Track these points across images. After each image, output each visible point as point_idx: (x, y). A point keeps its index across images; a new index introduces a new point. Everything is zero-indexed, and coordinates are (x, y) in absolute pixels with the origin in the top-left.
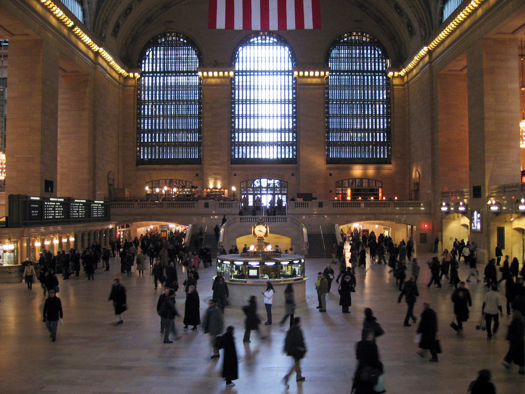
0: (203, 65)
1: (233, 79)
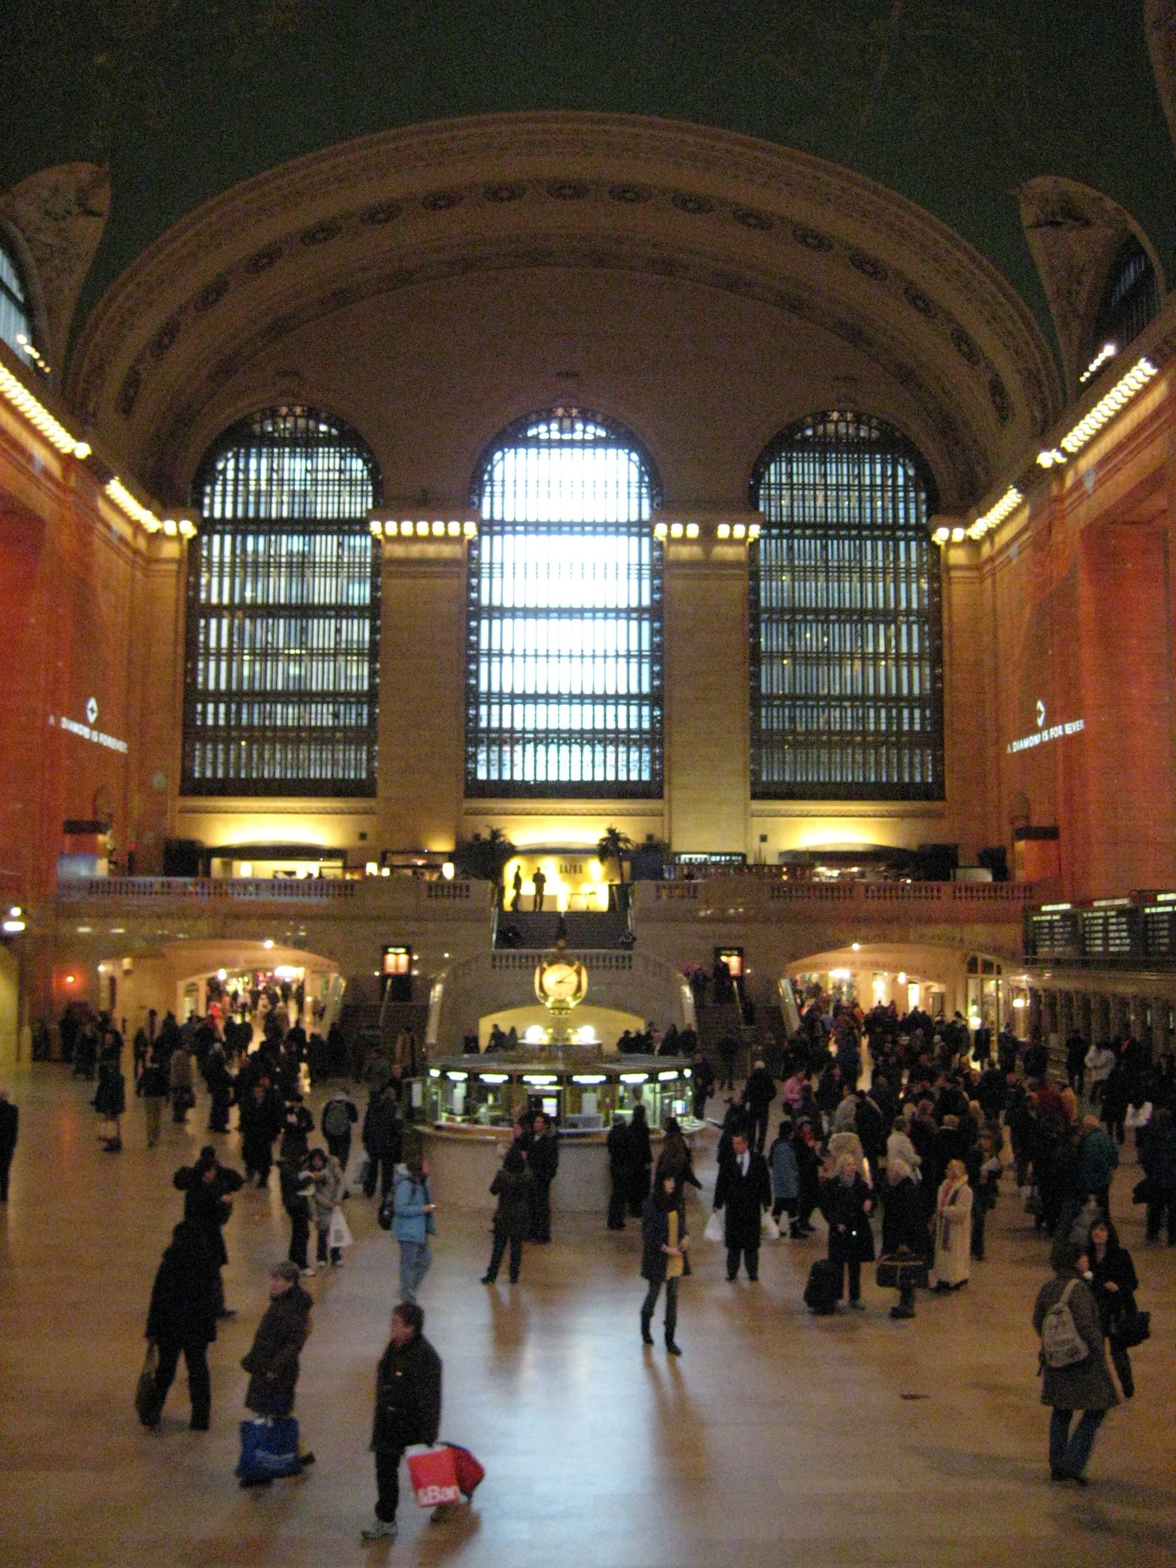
0: (385, 506)
1: (474, 545)
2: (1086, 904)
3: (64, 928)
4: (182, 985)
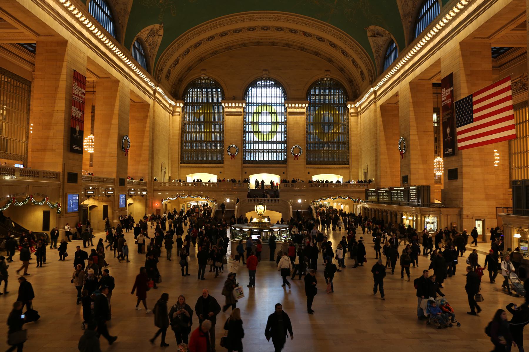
1: (245, 108)
2: (379, 189)
3: (155, 193)
4: (181, 205)
